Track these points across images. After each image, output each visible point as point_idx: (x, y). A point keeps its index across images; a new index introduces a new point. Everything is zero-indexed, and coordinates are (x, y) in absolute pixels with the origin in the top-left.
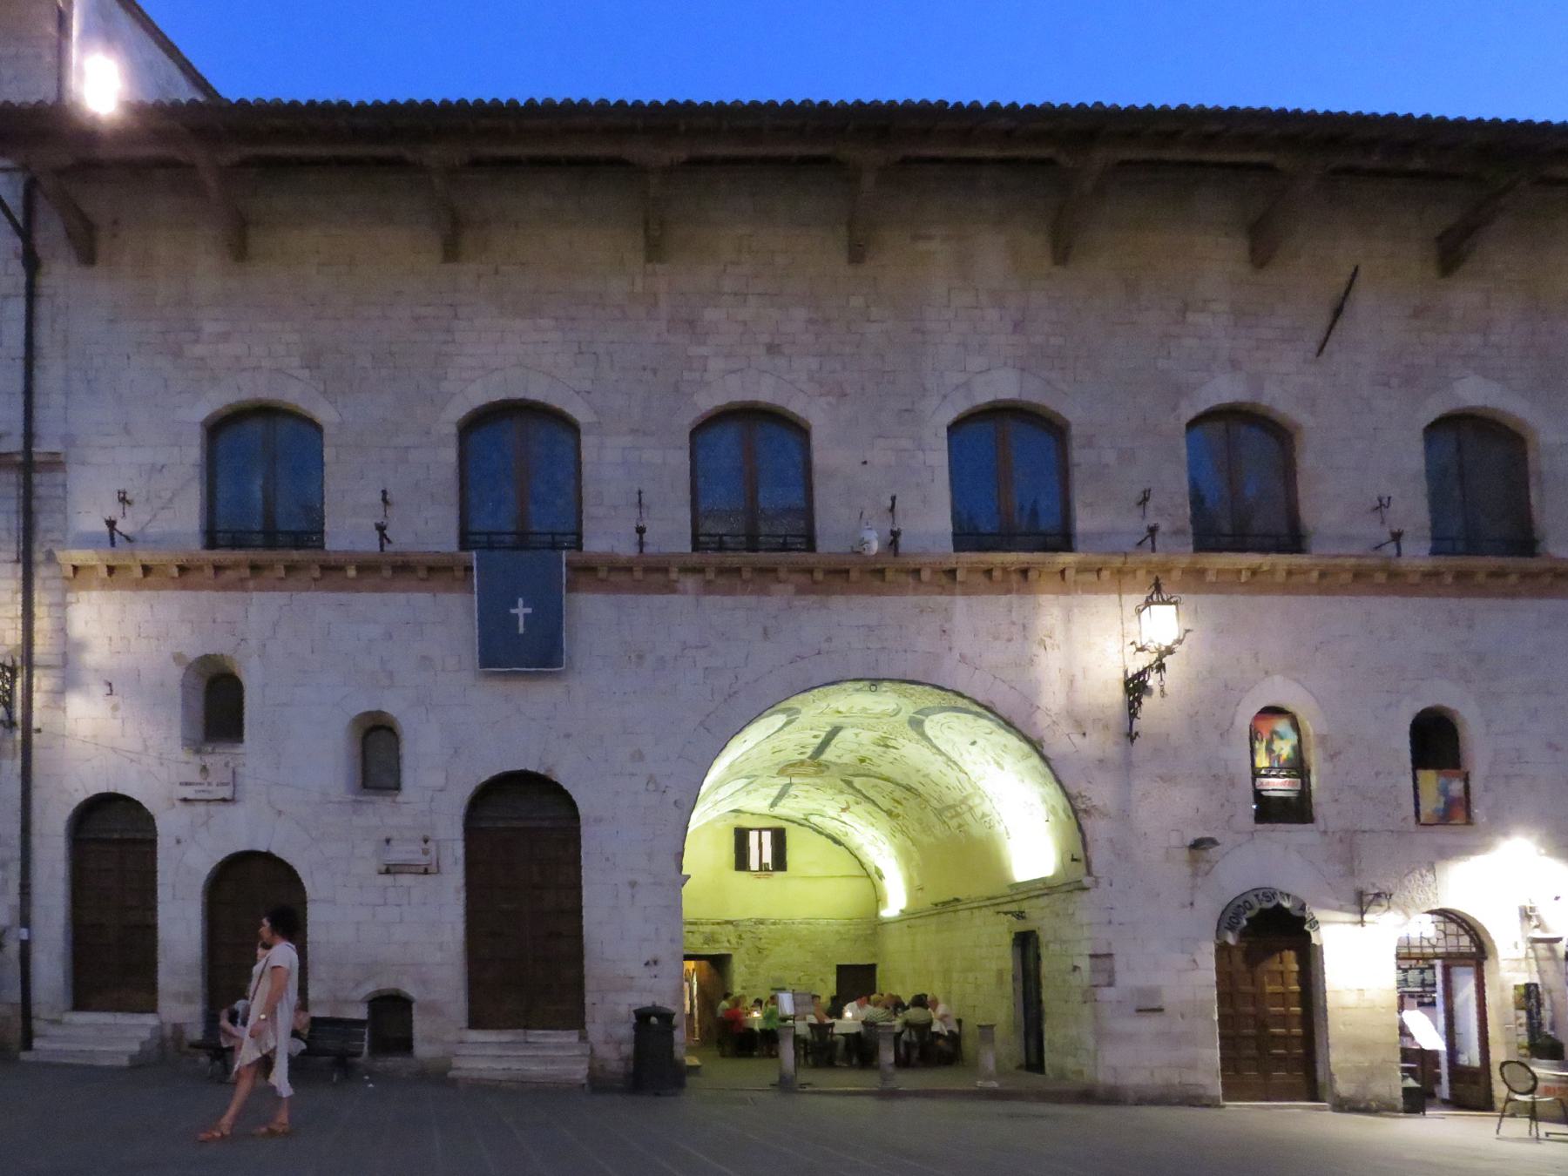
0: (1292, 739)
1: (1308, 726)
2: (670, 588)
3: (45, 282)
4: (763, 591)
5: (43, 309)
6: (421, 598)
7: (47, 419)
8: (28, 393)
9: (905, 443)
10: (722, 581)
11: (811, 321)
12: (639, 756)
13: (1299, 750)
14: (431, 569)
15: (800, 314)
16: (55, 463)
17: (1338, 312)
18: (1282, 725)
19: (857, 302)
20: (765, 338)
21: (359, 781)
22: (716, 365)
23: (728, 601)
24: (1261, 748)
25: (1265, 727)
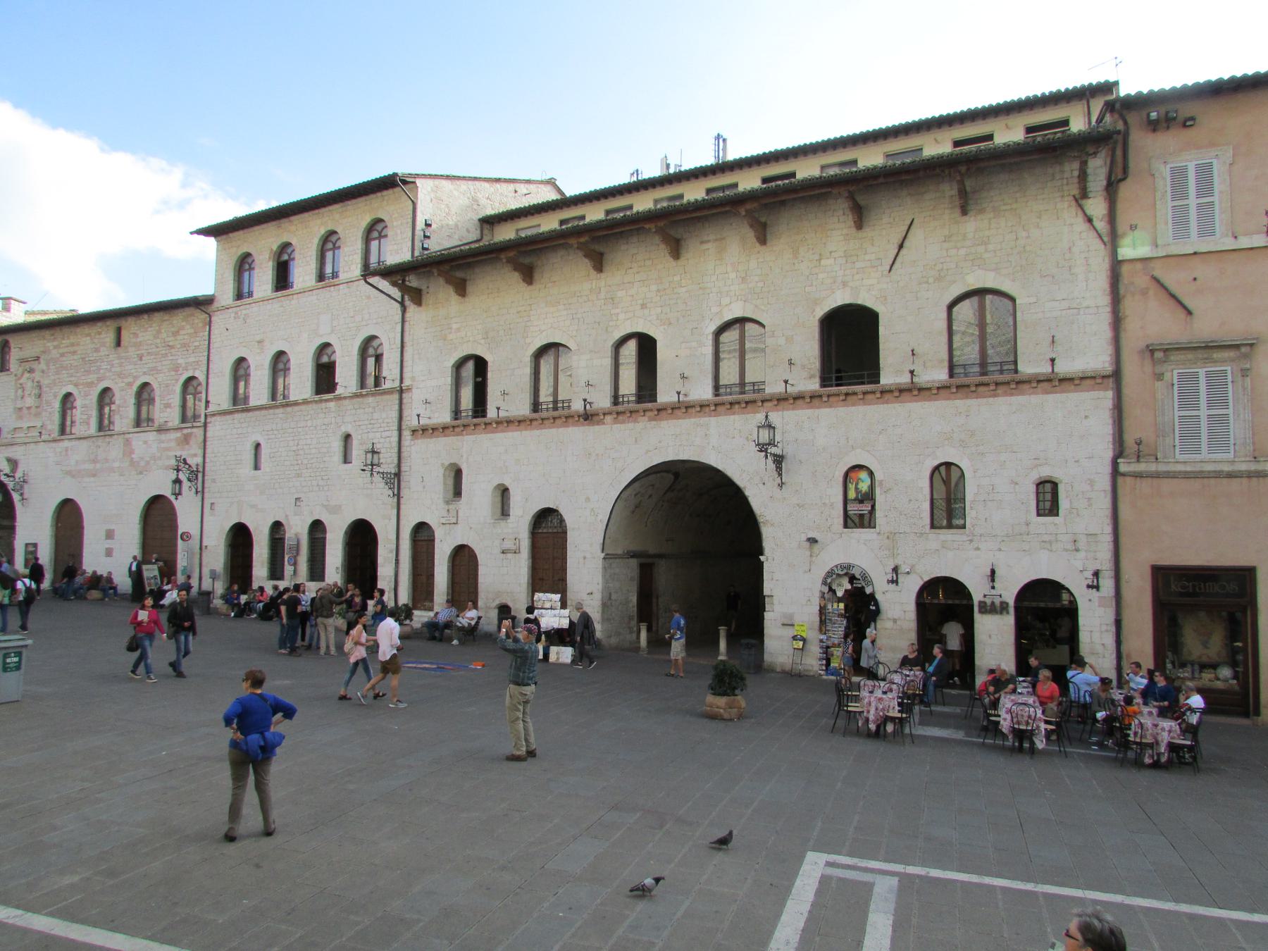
0: (868, 481)
1: (878, 476)
2: (601, 422)
3: (408, 315)
4: (636, 421)
5: (407, 325)
6: (516, 434)
7: (407, 375)
8: (402, 361)
9: (694, 344)
10: (620, 418)
11: (658, 291)
12: (588, 499)
13: (872, 487)
14: (519, 422)
15: (654, 288)
16: (409, 389)
17: (901, 247)
18: (863, 475)
19: (677, 278)
20: (640, 302)
21: (499, 511)
22: (622, 316)
23: (622, 426)
24: (851, 487)
25: (852, 475)
